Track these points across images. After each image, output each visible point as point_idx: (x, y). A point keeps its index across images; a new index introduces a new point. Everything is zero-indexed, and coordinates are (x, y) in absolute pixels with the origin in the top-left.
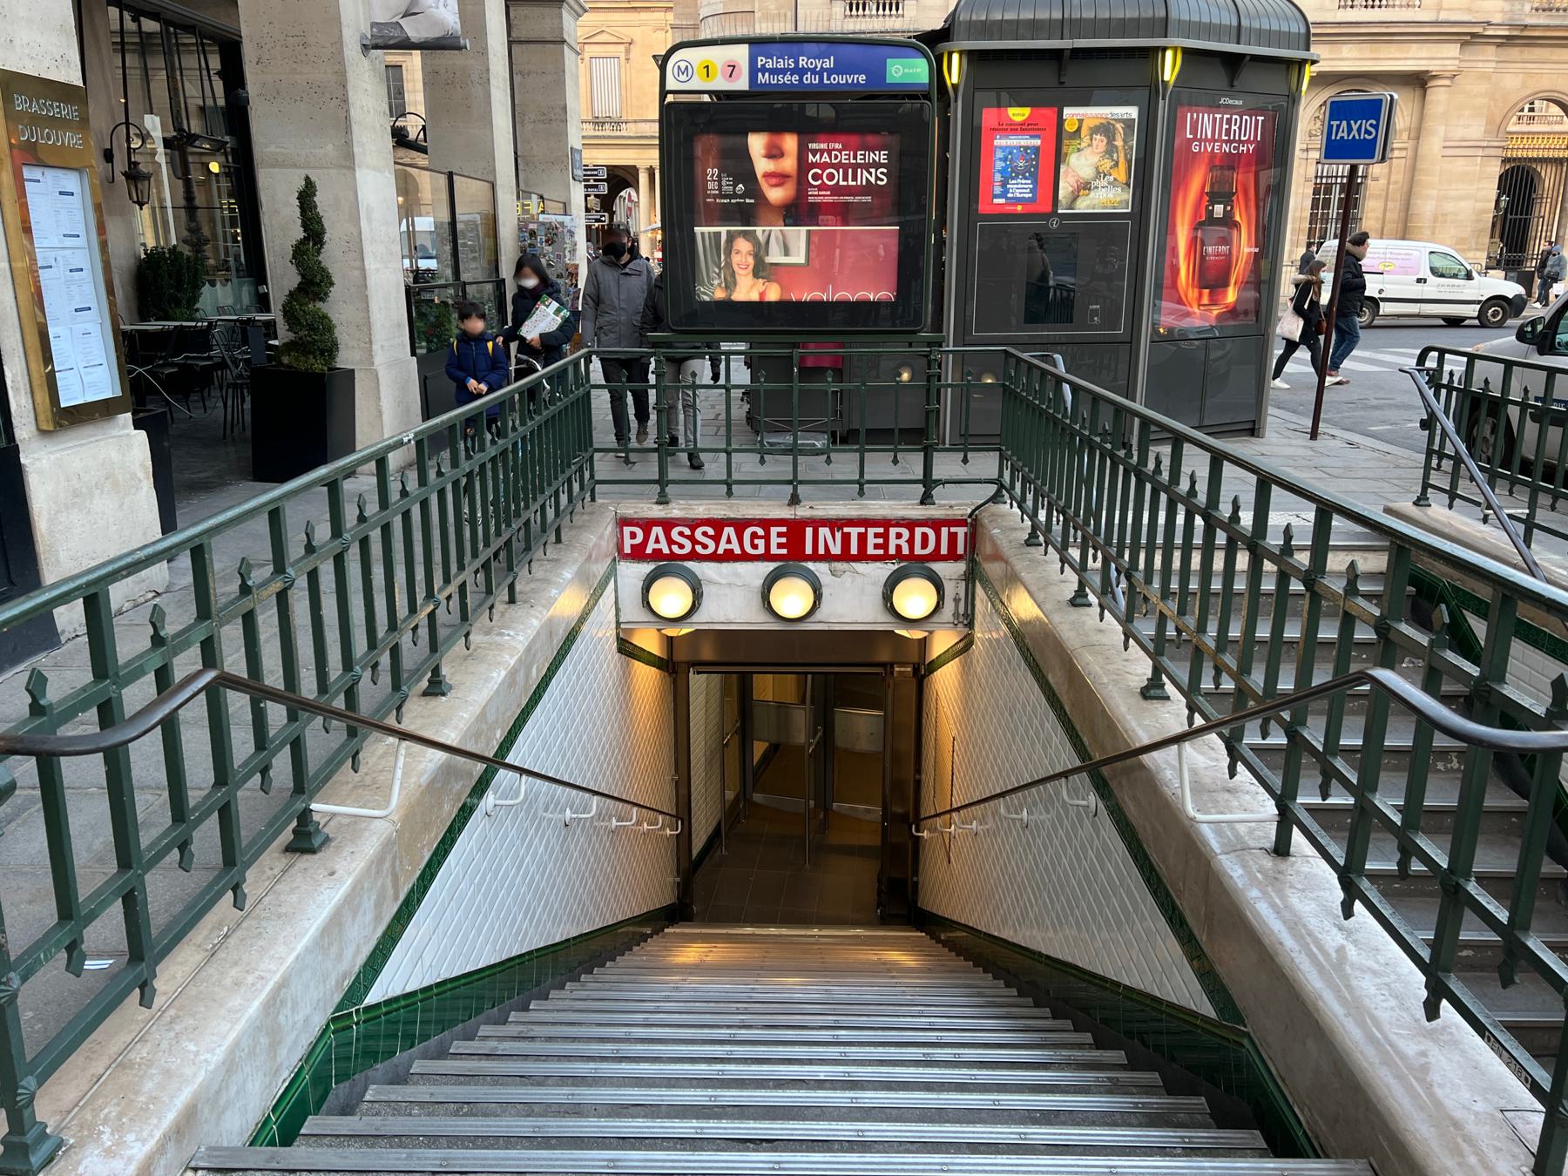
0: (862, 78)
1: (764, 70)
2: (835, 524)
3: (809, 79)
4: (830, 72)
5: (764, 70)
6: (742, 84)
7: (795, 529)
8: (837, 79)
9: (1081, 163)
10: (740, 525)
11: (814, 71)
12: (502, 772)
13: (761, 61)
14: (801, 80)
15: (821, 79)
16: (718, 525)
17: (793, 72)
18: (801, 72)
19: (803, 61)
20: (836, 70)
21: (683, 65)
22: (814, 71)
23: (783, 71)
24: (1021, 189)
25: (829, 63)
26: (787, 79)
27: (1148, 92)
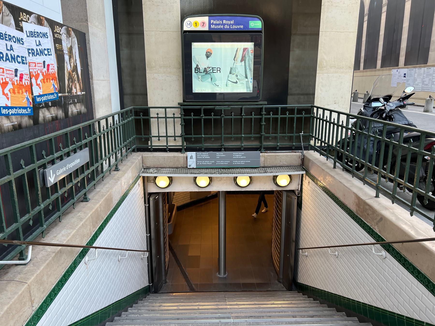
0: (242, 27)
1: (213, 24)
4: (232, 25)
5: (213, 24)
6: (206, 28)
8: (234, 27)
11: (228, 25)
12: (91, 249)
13: (212, 21)
14: (224, 27)
15: (230, 27)
18: (224, 25)
19: (224, 22)
20: (236, 24)
21: (189, 23)
22: (228, 25)
23: (219, 25)
25: (232, 22)
26: (220, 27)
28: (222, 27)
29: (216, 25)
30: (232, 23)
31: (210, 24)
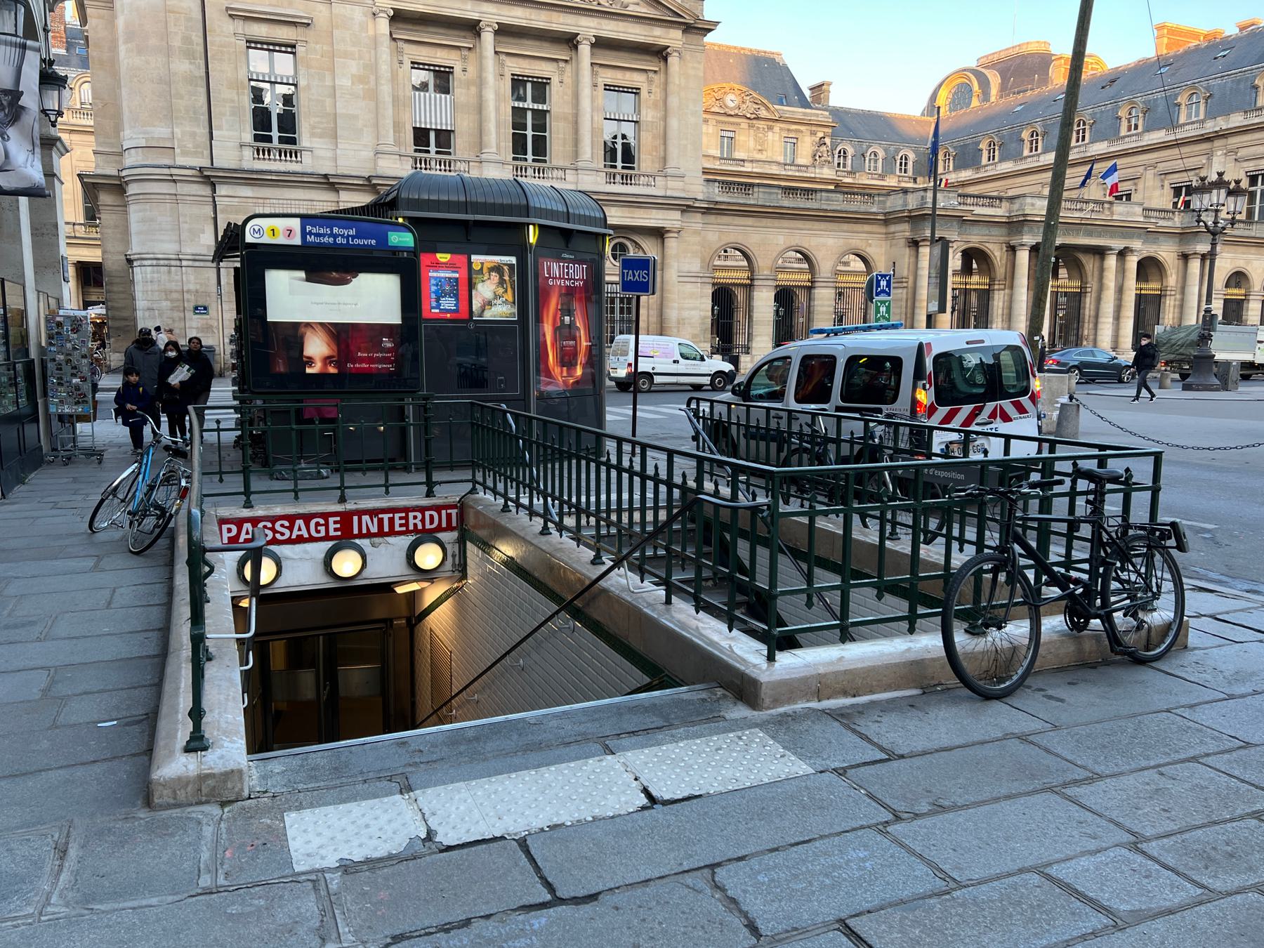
1: (310, 233)
2: (372, 513)
3: (339, 240)
6: (297, 240)
7: (346, 518)
8: (357, 241)
9: (485, 289)
10: (307, 518)
11: (343, 236)
13: (308, 228)
16: (292, 519)
17: (330, 236)
18: (335, 236)
19: (335, 230)
22: (343, 236)
23: (323, 235)
24: (448, 303)
26: (326, 240)
27: (520, 249)
28: (331, 240)
29: (317, 235)
30: (351, 233)
31: (304, 234)
